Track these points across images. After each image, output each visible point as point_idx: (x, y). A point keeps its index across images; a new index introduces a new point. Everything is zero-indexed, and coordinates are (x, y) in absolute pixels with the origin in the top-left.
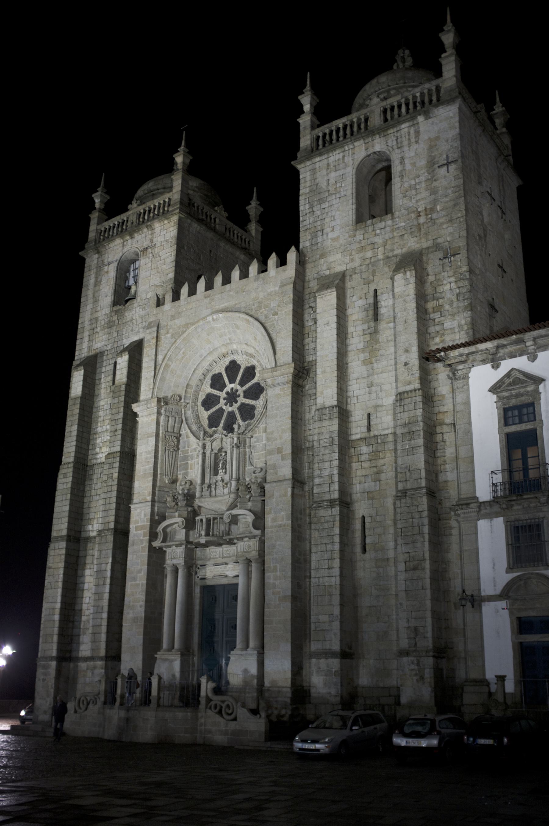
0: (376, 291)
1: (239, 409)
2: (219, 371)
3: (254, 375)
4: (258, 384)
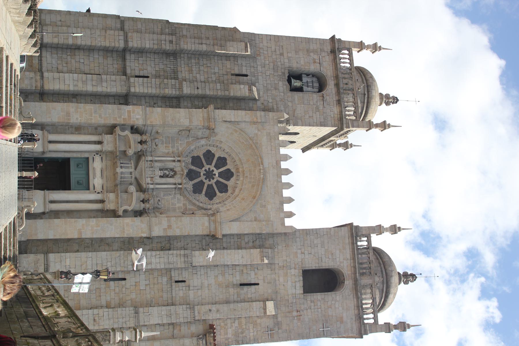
0: (258, 284)
1: (202, 181)
2: (228, 164)
3: (221, 192)
4: (215, 195)
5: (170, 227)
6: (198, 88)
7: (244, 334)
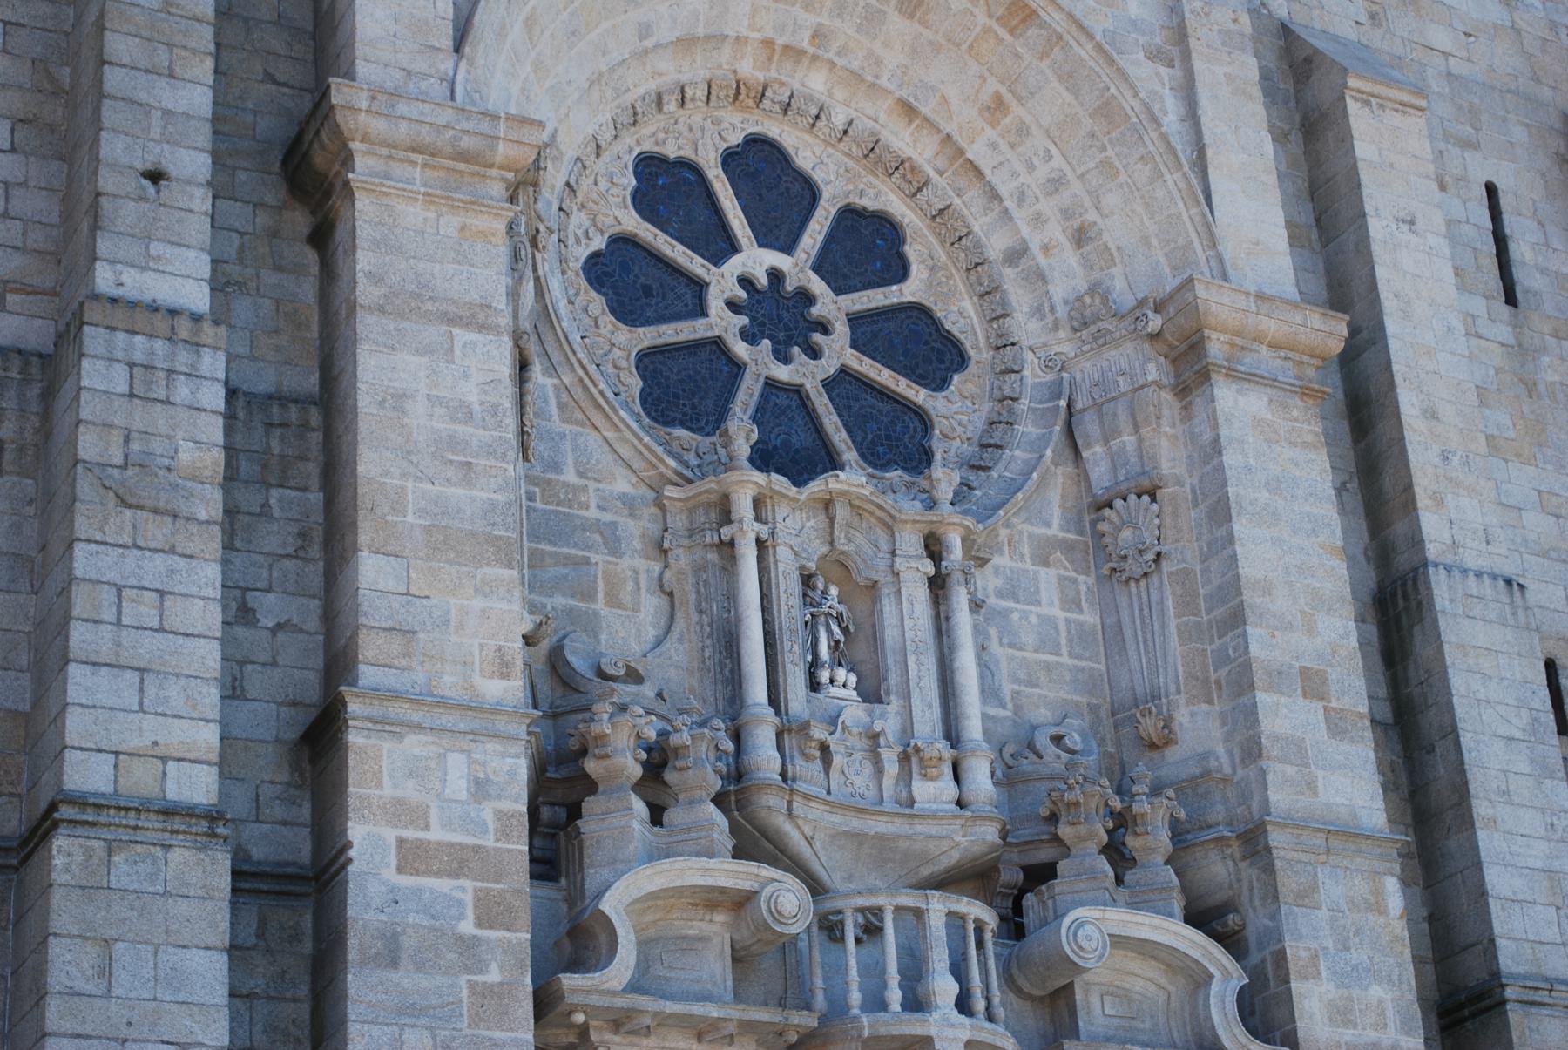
0: (1491, 190)
1: (829, 385)
2: (687, 153)
3: (899, 270)
4: (918, 311)
5: (1313, 684)
6: (155, 176)
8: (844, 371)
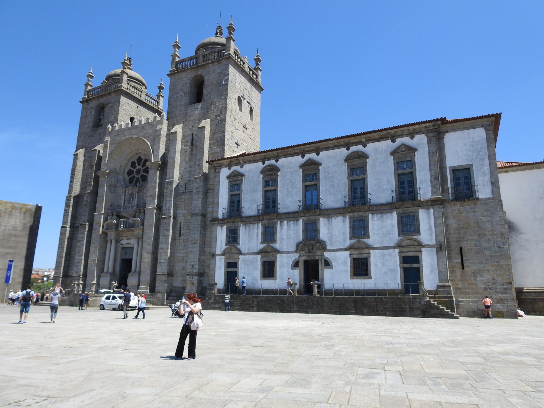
0: (193, 134)
7: (219, 140)
8: (142, 175)
